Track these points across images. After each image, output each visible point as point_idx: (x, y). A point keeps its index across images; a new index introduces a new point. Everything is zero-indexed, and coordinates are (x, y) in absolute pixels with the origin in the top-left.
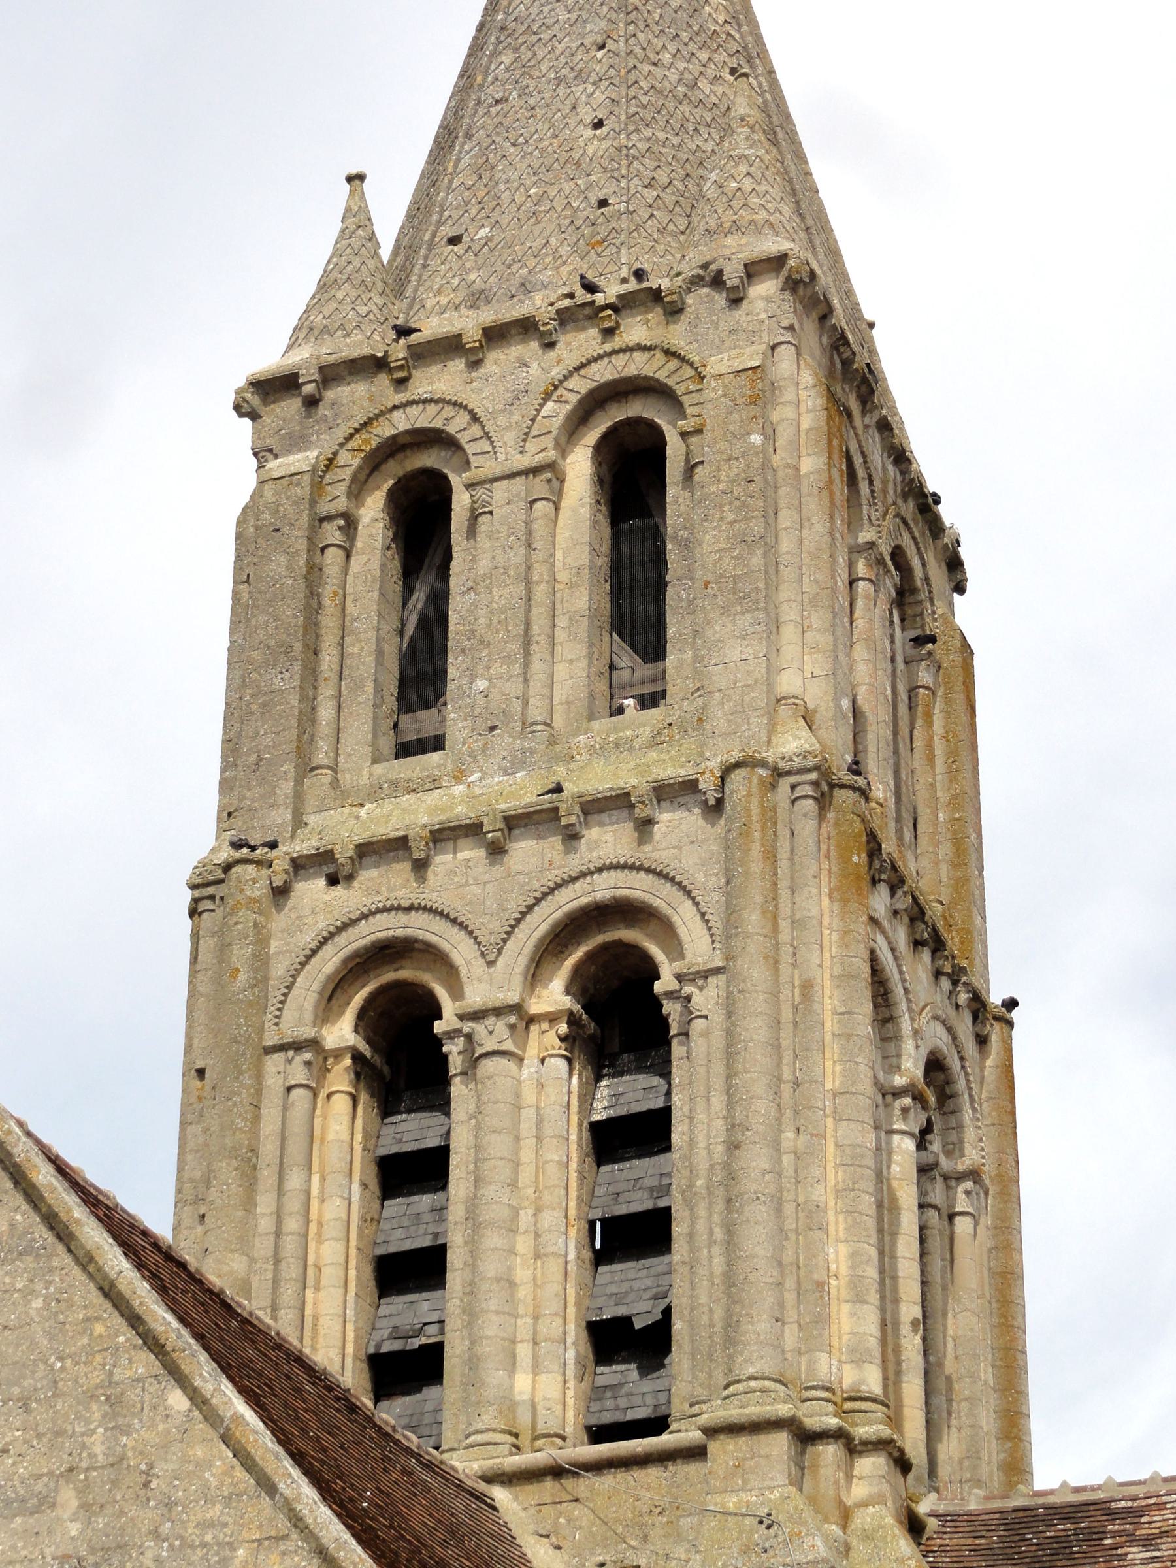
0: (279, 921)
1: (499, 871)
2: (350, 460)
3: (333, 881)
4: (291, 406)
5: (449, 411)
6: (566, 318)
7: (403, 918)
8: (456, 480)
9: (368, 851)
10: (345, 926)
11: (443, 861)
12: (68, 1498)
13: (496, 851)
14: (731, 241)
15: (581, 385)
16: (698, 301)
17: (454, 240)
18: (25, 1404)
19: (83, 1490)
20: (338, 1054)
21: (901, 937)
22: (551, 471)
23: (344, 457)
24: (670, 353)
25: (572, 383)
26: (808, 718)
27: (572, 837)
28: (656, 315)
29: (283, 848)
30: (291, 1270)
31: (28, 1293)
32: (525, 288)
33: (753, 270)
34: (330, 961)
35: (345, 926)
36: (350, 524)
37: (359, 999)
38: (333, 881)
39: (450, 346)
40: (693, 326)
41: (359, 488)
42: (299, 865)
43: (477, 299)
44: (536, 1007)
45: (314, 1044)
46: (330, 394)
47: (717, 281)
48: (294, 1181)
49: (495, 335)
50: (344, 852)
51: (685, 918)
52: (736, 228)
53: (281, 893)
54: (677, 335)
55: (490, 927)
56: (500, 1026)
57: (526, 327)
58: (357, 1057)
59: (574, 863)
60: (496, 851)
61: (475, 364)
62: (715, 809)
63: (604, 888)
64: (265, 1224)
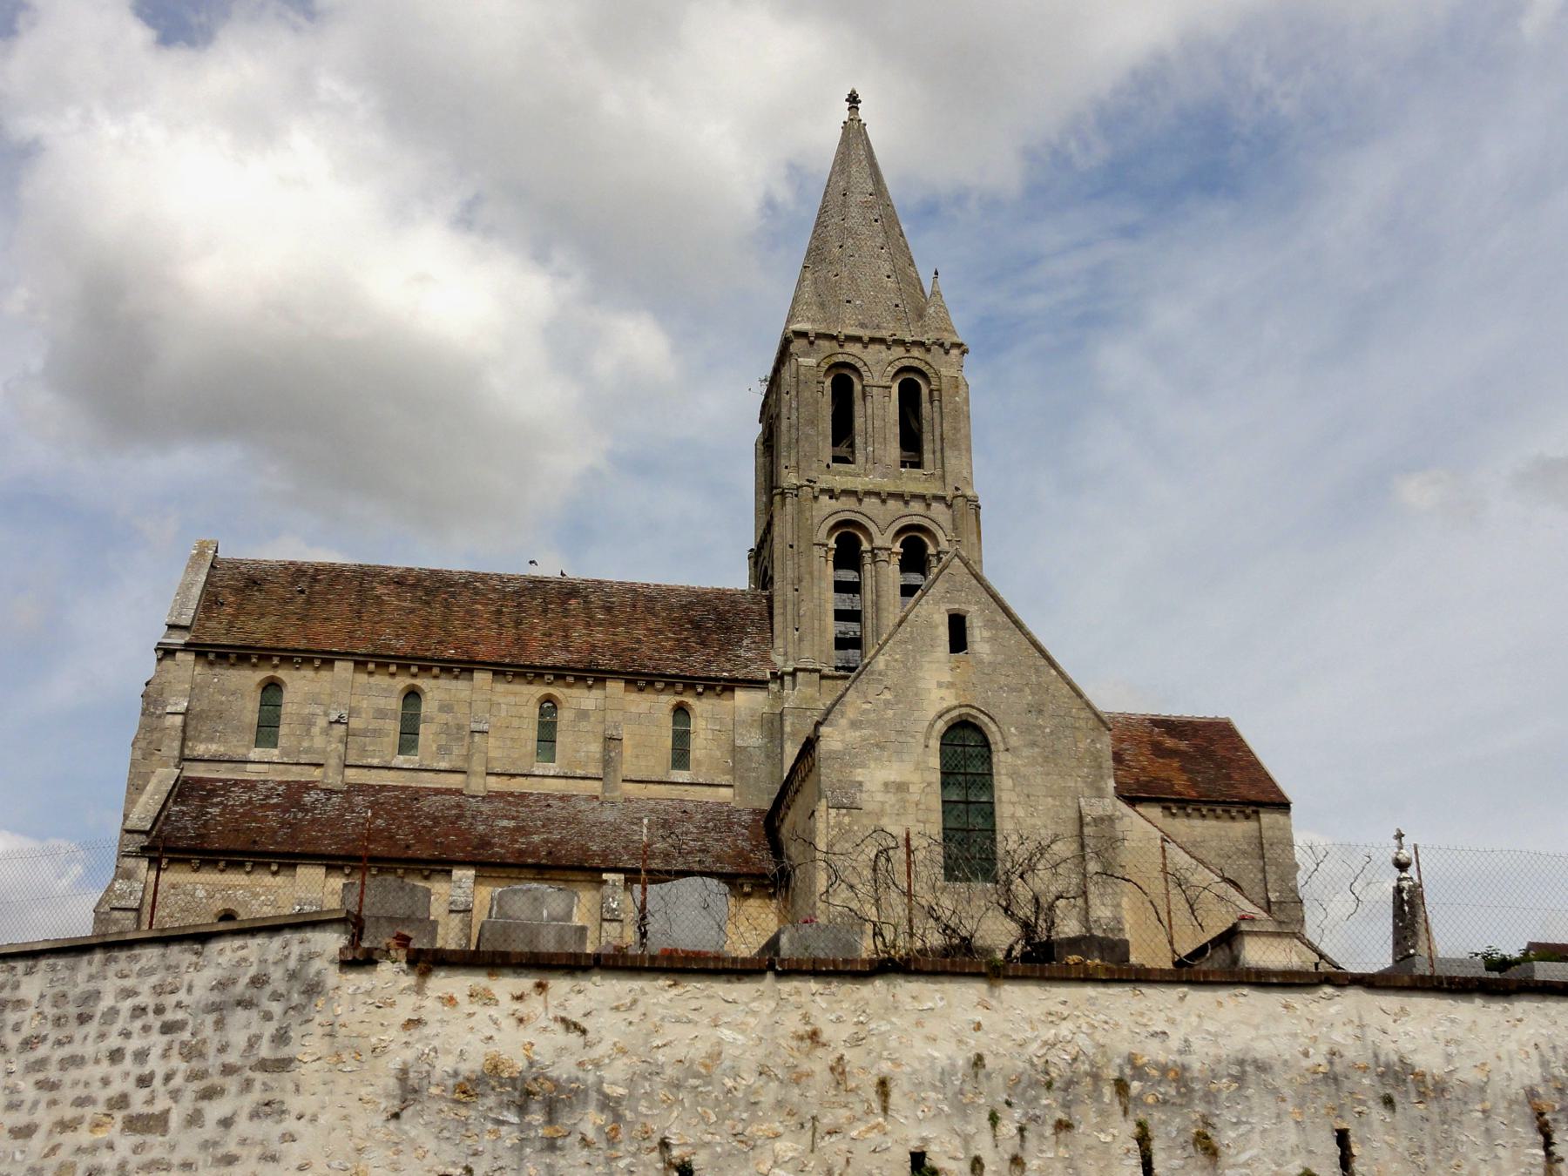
0: (815, 506)
1: (883, 508)
2: (825, 366)
3: (831, 498)
4: (804, 342)
5: (857, 360)
7: (854, 514)
8: (855, 380)
9: (846, 492)
10: (837, 512)
11: (866, 500)
12: (1027, 691)
13: (884, 501)
14: (945, 334)
15: (898, 365)
16: (935, 348)
17: (848, 302)
18: (1013, 665)
19: (1031, 689)
20: (831, 549)
23: (822, 364)
24: (927, 363)
25: (897, 363)
27: (907, 503)
28: (922, 350)
29: (818, 484)
31: (1010, 639)
32: (878, 327)
34: (832, 521)
35: (837, 512)
37: (836, 534)
38: (831, 498)
39: (858, 339)
40: (933, 357)
41: (826, 375)
42: (822, 491)
43: (863, 326)
45: (827, 545)
46: (816, 342)
47: (942, 345)
49: (873, 340)
50: (837, 491)
51: (940, 535)
52: (946, 330)
53: (816, 498)
54: (928, 358)
55: (882, 524)
56: (886, 553)
57: (882, 341)
60: (884, 501)
61: (866, 347)
62: (950, 506)
63: (916, 520)
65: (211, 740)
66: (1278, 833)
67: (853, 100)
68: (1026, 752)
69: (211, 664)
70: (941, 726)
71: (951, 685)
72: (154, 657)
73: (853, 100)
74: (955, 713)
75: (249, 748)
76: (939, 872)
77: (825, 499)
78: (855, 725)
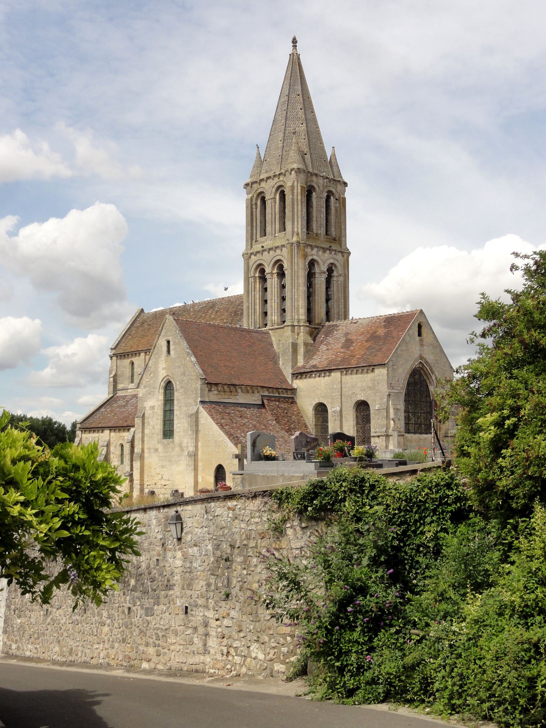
2: (255, 196)
6: (275, 176)
15: (276, 186)
21: (320, 253)
22: (274, 198)
26: (298, 234)
30: (253, 304)
33: (292, 170)
34: (255, 266)
36: (256, 204)
42: (251, 254)
44: (274, 272)
48: (253, 294)
53: (250, 257)
54: (285, 179)
57: (270, 177)
58: (259, 277)
59: (275, 254)
60: (269, 253)
64: (250, 299)
65: (122, 383)
66: (381, 377)
67: (294, 41)
68: (181, 391)
69: (120, 359)
70: (163, 384)
71: (165, 368)
72: (109, 358)
73: (294, 41)
74: (166, 379)
75: (129, 384)
76: (161, 436)
77: (253, 256)
78: (145, 387)
